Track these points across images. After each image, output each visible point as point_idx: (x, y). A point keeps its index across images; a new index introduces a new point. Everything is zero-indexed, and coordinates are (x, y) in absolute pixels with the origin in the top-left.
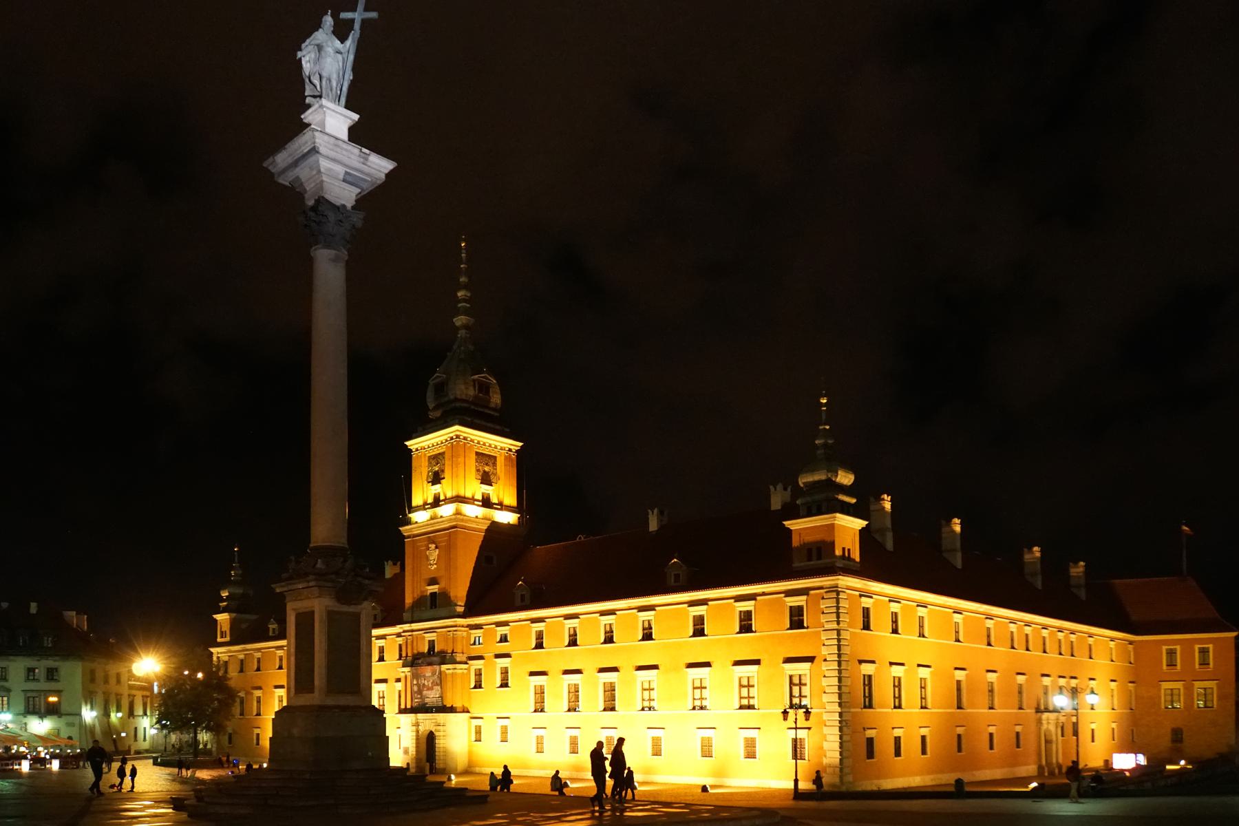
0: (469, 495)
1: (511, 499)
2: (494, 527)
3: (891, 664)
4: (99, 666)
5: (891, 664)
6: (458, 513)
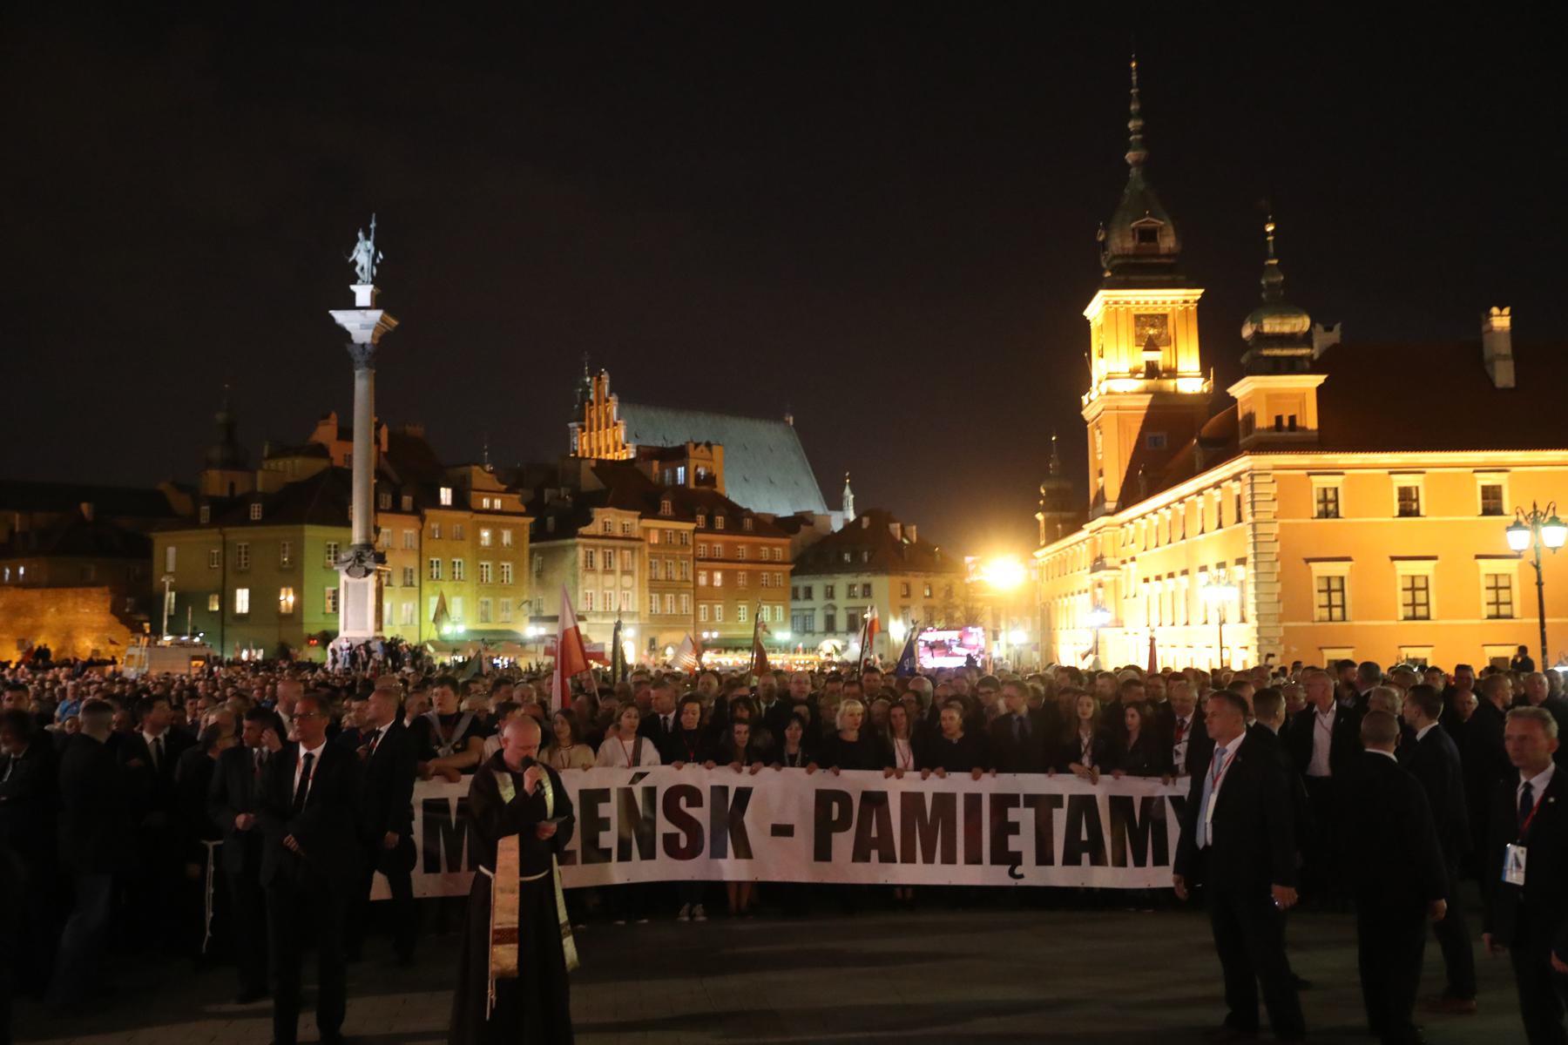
3: (1393, 559)
4: (940, 581)
5: (1393, 559)
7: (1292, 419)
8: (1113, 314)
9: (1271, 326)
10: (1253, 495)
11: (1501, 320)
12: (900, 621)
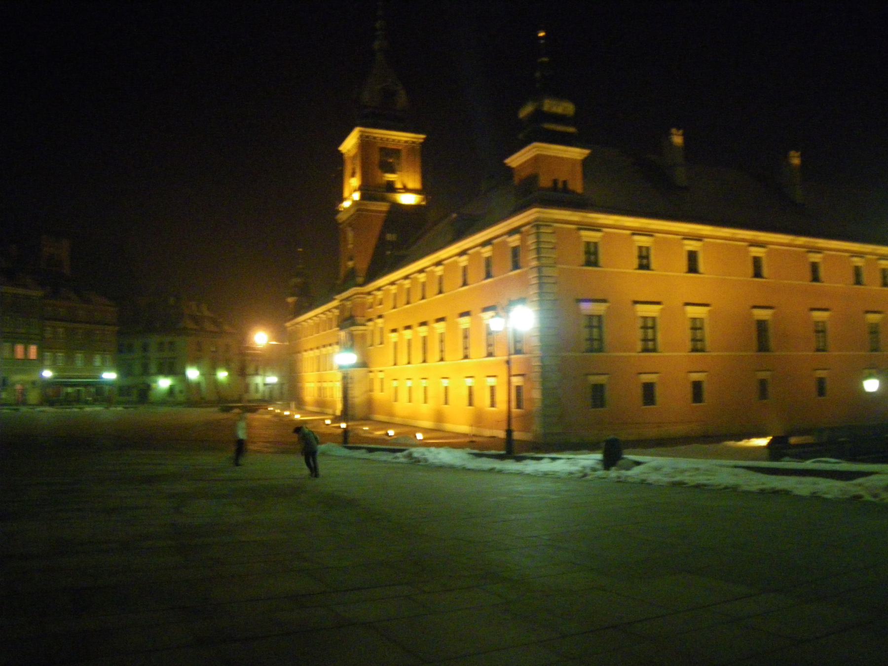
1: (414, 182)
3: (636, 302)
7: (565, 182)
10: (538, 242)
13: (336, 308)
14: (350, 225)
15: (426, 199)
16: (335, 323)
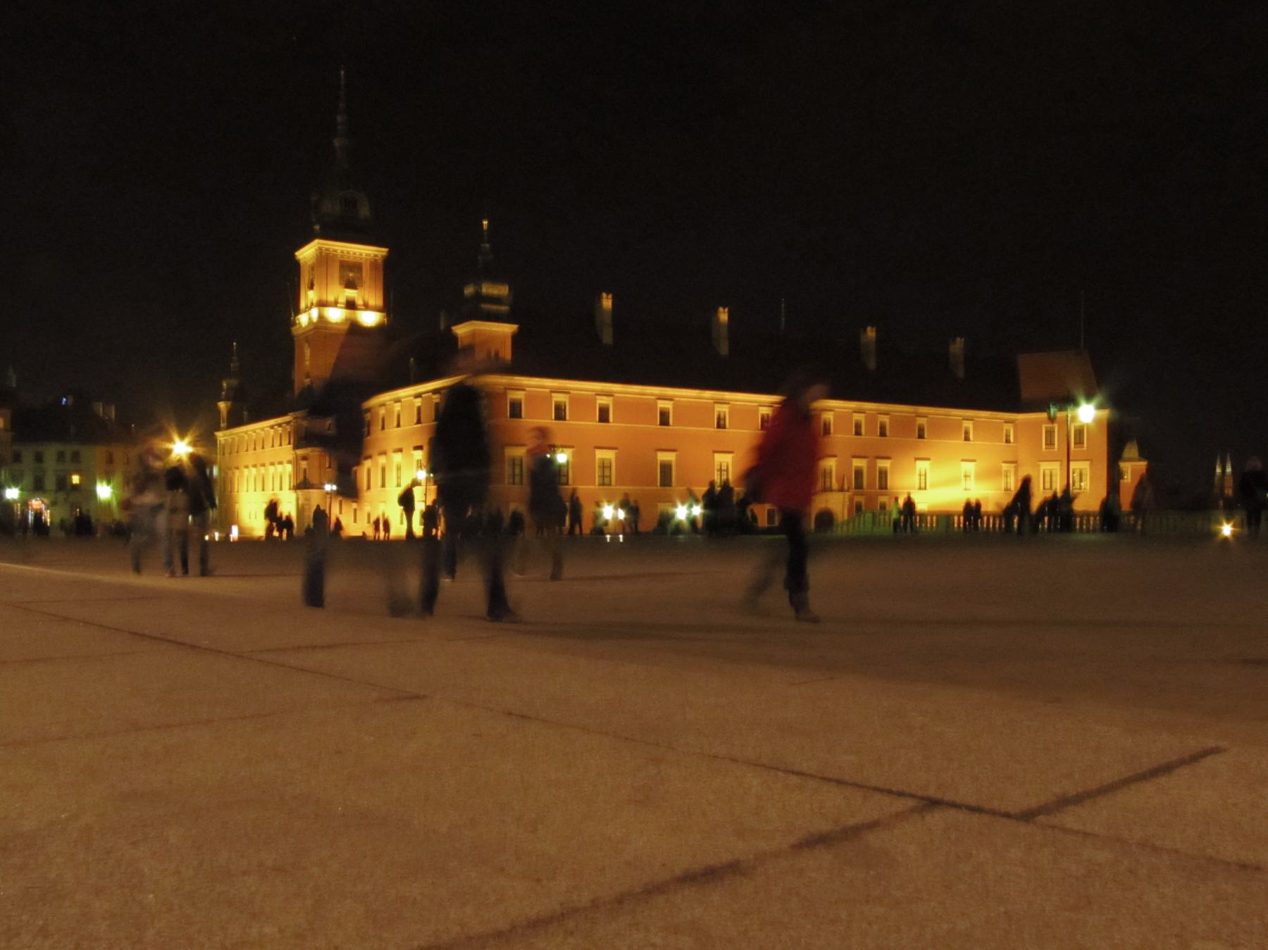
0: (331, 298)
1: (376, 299)
2: (354, 329)
6: (321, 317)
7: (497, 354)
8: (323, 259)
9: (488, 289)
11: (723, 316)
12: (105, 484)
13: (288, 423)
14: (307, 341)
15: (388, 315)
16: (285, 441)
